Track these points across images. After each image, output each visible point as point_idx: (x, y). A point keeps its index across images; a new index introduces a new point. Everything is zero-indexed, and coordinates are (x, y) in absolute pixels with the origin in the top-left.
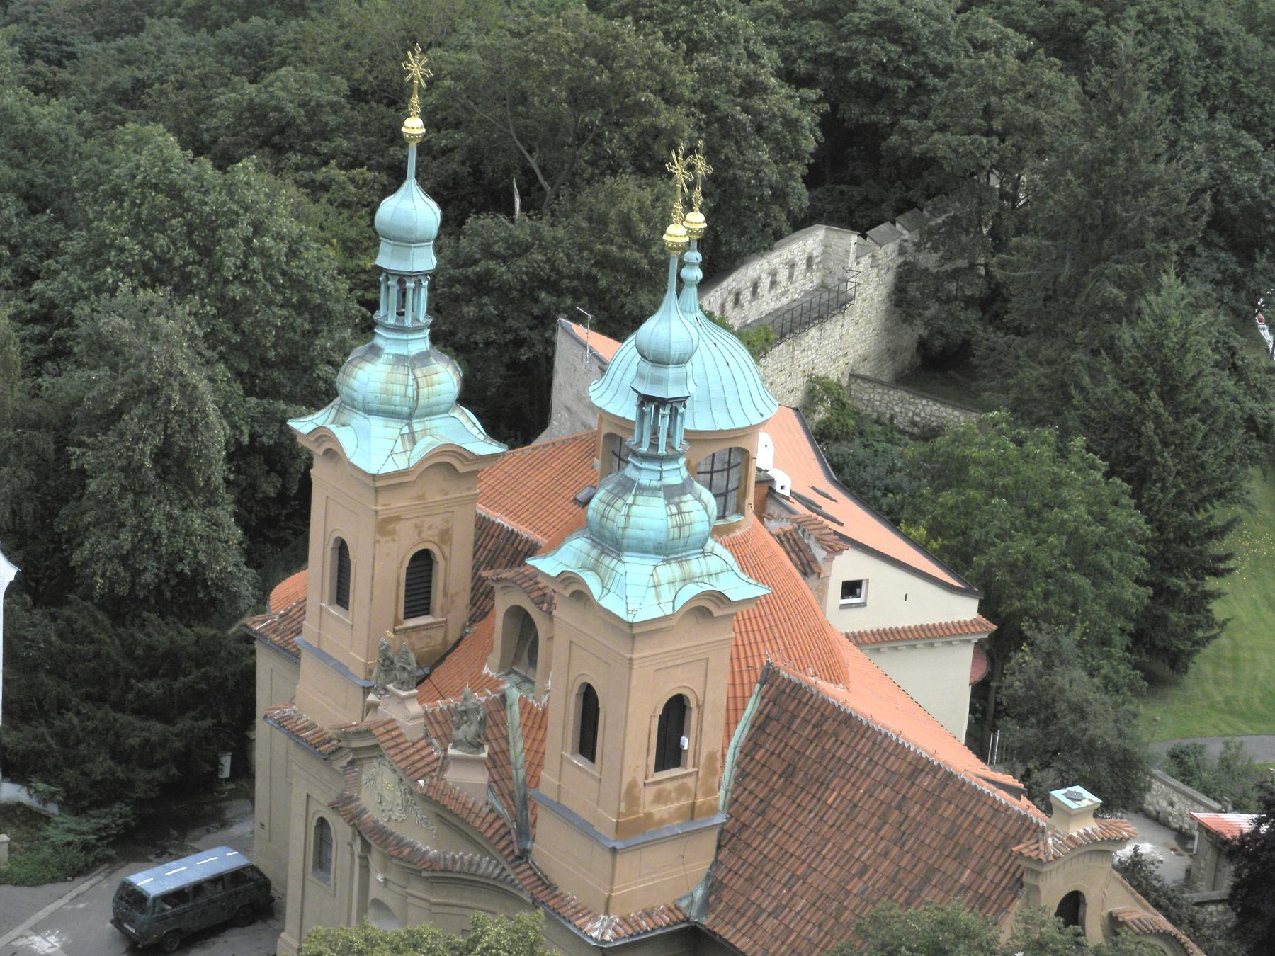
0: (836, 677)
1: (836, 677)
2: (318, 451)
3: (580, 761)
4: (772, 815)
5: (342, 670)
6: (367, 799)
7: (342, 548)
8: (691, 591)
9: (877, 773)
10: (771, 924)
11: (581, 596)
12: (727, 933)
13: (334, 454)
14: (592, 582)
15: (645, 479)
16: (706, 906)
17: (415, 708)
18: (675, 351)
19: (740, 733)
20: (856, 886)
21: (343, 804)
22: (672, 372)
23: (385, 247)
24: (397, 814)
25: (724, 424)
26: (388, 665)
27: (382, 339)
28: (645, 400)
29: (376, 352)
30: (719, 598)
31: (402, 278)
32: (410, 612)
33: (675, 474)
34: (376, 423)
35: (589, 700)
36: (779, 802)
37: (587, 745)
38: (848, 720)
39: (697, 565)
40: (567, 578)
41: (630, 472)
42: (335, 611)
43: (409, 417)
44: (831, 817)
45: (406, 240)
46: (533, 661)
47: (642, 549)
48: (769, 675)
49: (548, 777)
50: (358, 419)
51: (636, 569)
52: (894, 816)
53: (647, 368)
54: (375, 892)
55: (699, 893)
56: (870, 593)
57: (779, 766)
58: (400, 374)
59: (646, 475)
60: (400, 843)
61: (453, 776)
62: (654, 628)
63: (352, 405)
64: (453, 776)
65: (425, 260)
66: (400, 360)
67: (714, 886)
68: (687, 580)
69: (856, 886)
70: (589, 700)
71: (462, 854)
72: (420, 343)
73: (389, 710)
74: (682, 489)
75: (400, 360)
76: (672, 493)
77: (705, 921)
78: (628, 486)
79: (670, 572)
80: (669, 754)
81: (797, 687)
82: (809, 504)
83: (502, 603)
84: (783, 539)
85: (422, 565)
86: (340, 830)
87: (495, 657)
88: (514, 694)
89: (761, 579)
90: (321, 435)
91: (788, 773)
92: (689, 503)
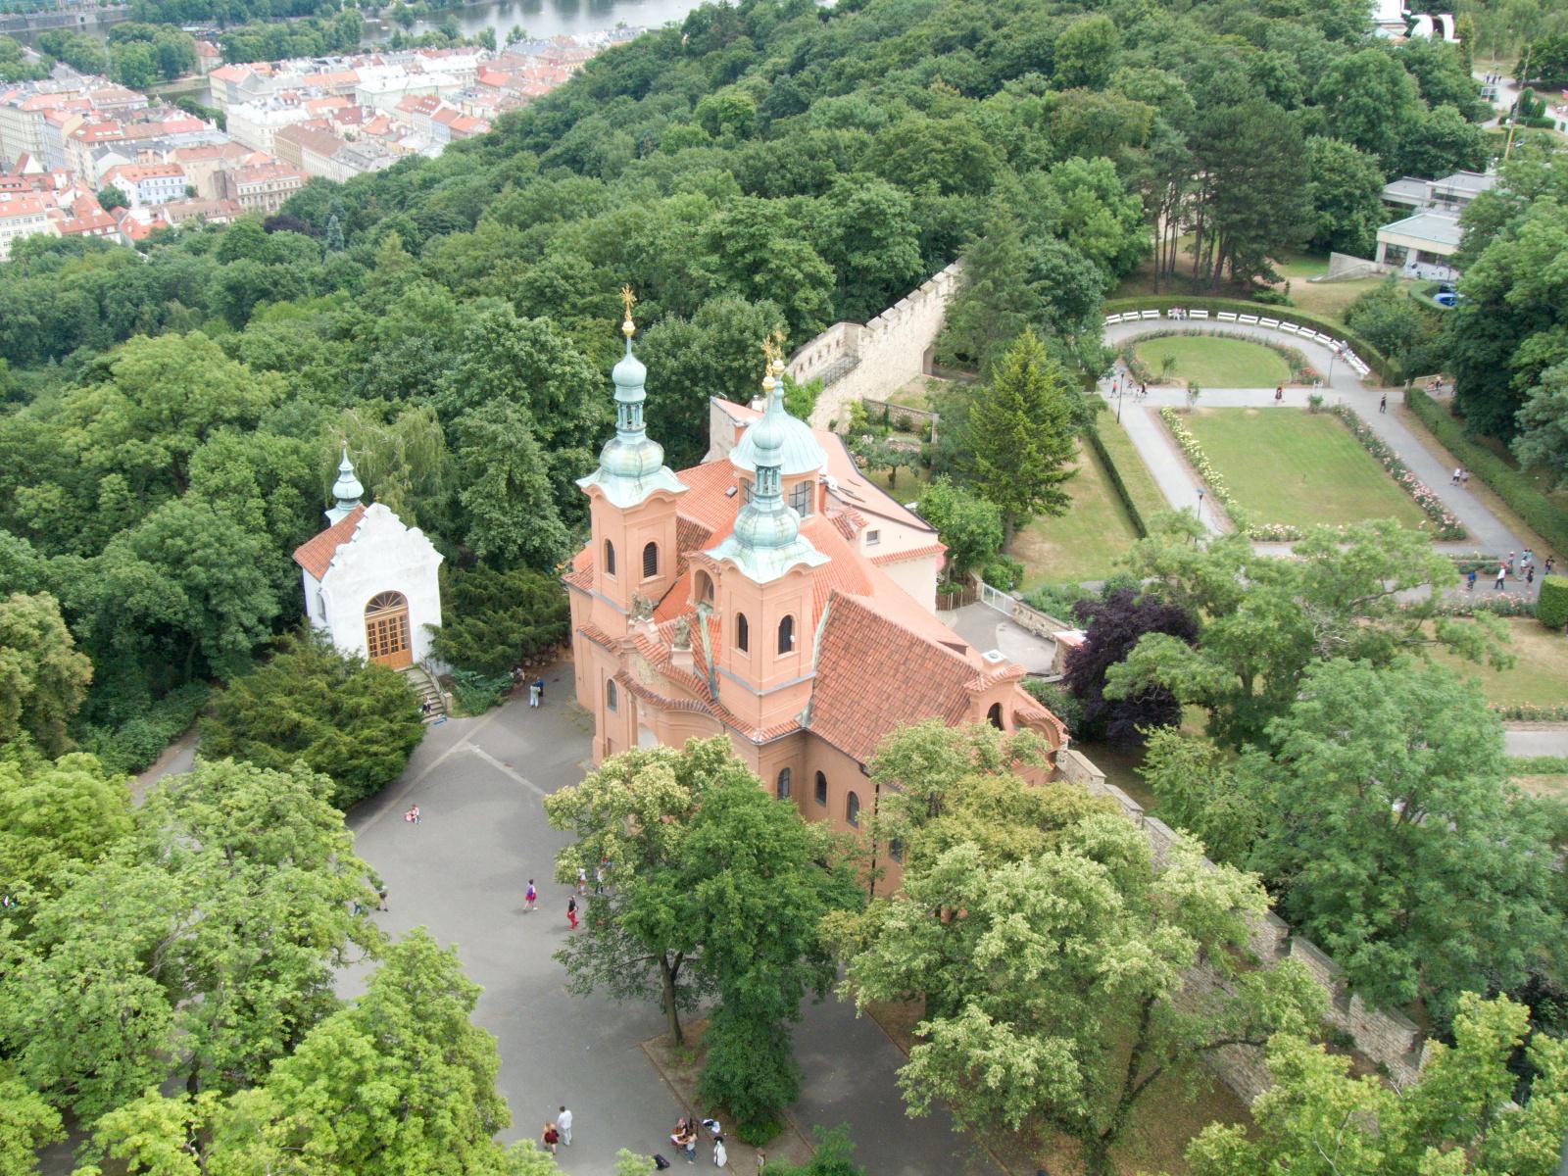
0: (866, 591)
1: (866, 591)
2: (593, 496)
3: (740, 651)
4: (840, 670)
5: (613, 606)
6: (632, 673)
7: (609, 544)
8: (790, 565)
9: (893, 647)
10: (842, 727)
11: (734, 569)
12: (820, 732)
13: (600, 497)
14: (739, 563)
15: (762, 508)
16: (809, 719)
17: (653, 628)
18: (773, 442)
19: (820, 628)
20: (885, 706)
21: (621, 675)
22: (772, 453)
23: (618, 389)
24: (649, 681)
25: (800, 470)
26: (637, 604)
27: (620, 436)
28: (759, 468)
29: (618, 443)
30: (805, 566)
31: (629, 406)
32: (646, 575)
33: (778, 504)
34: (622, 481)
35: (742, 621)
36: (843, 663)
37: (743, 643)
38: (876, 619)
39: (792, 549)
40: (726, 561)
41: (754, 505)
42: (608, 575)
43: (638, 476)
44: (870, 670)
45: (629, 386)
46: (711, 596)
47: (763, 544)
48: (834, 596)
49: (724, 660)
50: (612, 479)
51: (760, 555)
52: (902, 669)
53: (759, 451)
54: (641, 719)
55: (806, 712)
56: (882, 536)
57: (842, 644)
58: (632, 454)
59: (763, 506)
60: (651, 696)
61: (676, 662)
62: (773, 585)
63: (607, 471)
64: (676, 662)
65: (641, 395)
66: (633, 446)
67: (812, 708)
68: (787, 558)
69: (885, 706)
70: (742, 621)
71: (684, 699)
72: (642, 437)
73: (639, 629)
74: (782, 511)
75: (633, 446)
76: (776, 514)
77: (810, 727)
78: (754, 512)
79: (779, 554)
80: (785, 645)
81: (848, 602)
82: (848, 493)
83: (693, 569)
84: (835, 521)
85: (651, 550)
86: (618, 686)
87: (692, 596)
88: (703, 615)
89: (827, 553)
90: (594, 488)
91: (846, 649)
92: (785, 518)
